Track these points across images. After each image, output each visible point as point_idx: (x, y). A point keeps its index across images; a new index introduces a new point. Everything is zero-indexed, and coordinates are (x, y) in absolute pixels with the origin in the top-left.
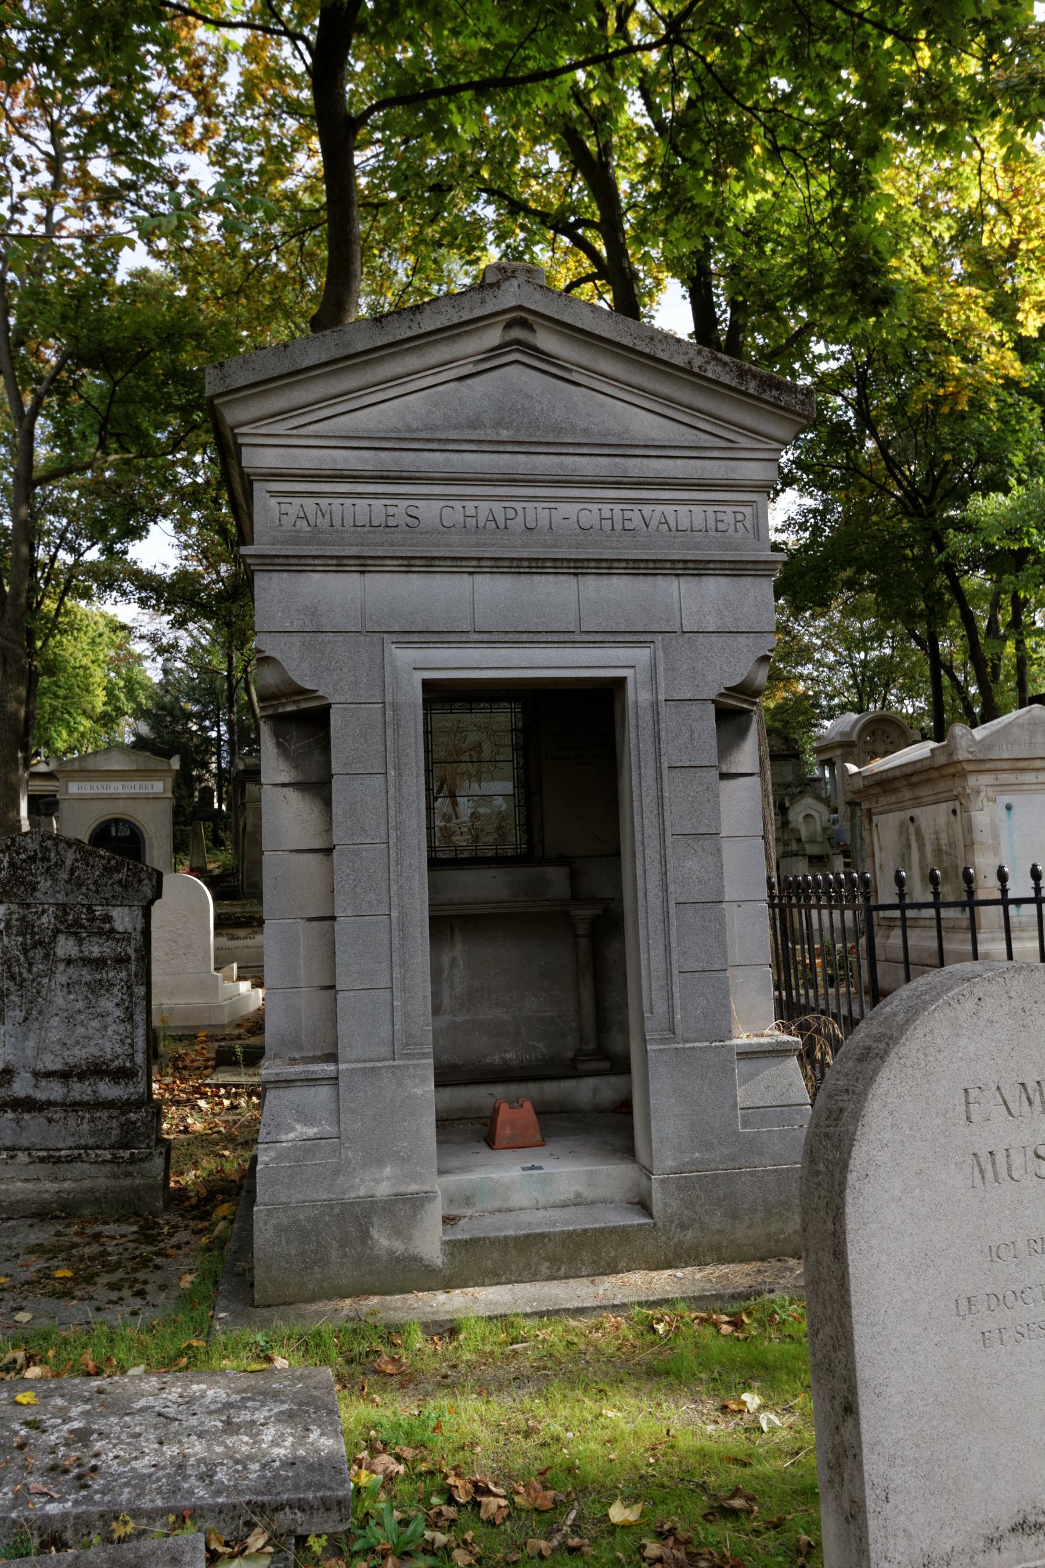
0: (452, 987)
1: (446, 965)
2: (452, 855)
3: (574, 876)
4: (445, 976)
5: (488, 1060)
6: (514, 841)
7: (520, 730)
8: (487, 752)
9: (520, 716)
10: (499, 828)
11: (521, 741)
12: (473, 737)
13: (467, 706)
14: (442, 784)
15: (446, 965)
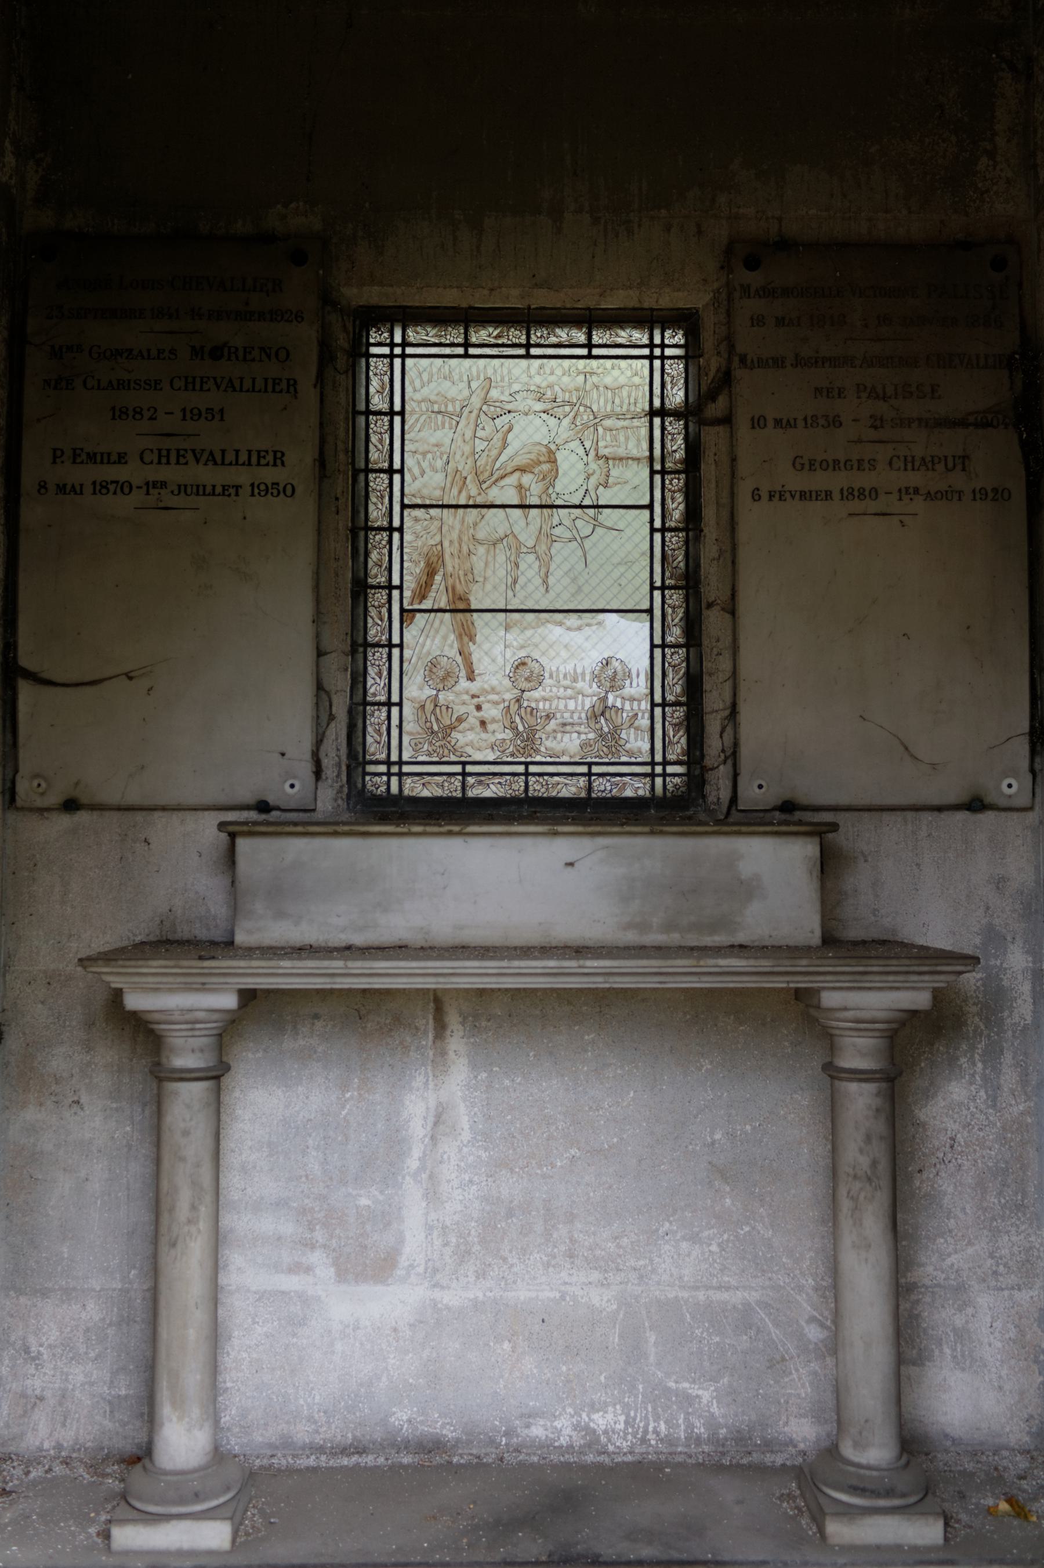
0: (433, 1196)
1: (418, 1129)
2: (452, 788)
3: (830, 864)
4: (413, 1163)
5: (538, 1431)
6: (643, 745)
7: (676, 414)
9: (676, 369)
10: (601, 711)
11: (677, 446)
12: (530, 432)
13: (517, 335)
15: (418, 1129)
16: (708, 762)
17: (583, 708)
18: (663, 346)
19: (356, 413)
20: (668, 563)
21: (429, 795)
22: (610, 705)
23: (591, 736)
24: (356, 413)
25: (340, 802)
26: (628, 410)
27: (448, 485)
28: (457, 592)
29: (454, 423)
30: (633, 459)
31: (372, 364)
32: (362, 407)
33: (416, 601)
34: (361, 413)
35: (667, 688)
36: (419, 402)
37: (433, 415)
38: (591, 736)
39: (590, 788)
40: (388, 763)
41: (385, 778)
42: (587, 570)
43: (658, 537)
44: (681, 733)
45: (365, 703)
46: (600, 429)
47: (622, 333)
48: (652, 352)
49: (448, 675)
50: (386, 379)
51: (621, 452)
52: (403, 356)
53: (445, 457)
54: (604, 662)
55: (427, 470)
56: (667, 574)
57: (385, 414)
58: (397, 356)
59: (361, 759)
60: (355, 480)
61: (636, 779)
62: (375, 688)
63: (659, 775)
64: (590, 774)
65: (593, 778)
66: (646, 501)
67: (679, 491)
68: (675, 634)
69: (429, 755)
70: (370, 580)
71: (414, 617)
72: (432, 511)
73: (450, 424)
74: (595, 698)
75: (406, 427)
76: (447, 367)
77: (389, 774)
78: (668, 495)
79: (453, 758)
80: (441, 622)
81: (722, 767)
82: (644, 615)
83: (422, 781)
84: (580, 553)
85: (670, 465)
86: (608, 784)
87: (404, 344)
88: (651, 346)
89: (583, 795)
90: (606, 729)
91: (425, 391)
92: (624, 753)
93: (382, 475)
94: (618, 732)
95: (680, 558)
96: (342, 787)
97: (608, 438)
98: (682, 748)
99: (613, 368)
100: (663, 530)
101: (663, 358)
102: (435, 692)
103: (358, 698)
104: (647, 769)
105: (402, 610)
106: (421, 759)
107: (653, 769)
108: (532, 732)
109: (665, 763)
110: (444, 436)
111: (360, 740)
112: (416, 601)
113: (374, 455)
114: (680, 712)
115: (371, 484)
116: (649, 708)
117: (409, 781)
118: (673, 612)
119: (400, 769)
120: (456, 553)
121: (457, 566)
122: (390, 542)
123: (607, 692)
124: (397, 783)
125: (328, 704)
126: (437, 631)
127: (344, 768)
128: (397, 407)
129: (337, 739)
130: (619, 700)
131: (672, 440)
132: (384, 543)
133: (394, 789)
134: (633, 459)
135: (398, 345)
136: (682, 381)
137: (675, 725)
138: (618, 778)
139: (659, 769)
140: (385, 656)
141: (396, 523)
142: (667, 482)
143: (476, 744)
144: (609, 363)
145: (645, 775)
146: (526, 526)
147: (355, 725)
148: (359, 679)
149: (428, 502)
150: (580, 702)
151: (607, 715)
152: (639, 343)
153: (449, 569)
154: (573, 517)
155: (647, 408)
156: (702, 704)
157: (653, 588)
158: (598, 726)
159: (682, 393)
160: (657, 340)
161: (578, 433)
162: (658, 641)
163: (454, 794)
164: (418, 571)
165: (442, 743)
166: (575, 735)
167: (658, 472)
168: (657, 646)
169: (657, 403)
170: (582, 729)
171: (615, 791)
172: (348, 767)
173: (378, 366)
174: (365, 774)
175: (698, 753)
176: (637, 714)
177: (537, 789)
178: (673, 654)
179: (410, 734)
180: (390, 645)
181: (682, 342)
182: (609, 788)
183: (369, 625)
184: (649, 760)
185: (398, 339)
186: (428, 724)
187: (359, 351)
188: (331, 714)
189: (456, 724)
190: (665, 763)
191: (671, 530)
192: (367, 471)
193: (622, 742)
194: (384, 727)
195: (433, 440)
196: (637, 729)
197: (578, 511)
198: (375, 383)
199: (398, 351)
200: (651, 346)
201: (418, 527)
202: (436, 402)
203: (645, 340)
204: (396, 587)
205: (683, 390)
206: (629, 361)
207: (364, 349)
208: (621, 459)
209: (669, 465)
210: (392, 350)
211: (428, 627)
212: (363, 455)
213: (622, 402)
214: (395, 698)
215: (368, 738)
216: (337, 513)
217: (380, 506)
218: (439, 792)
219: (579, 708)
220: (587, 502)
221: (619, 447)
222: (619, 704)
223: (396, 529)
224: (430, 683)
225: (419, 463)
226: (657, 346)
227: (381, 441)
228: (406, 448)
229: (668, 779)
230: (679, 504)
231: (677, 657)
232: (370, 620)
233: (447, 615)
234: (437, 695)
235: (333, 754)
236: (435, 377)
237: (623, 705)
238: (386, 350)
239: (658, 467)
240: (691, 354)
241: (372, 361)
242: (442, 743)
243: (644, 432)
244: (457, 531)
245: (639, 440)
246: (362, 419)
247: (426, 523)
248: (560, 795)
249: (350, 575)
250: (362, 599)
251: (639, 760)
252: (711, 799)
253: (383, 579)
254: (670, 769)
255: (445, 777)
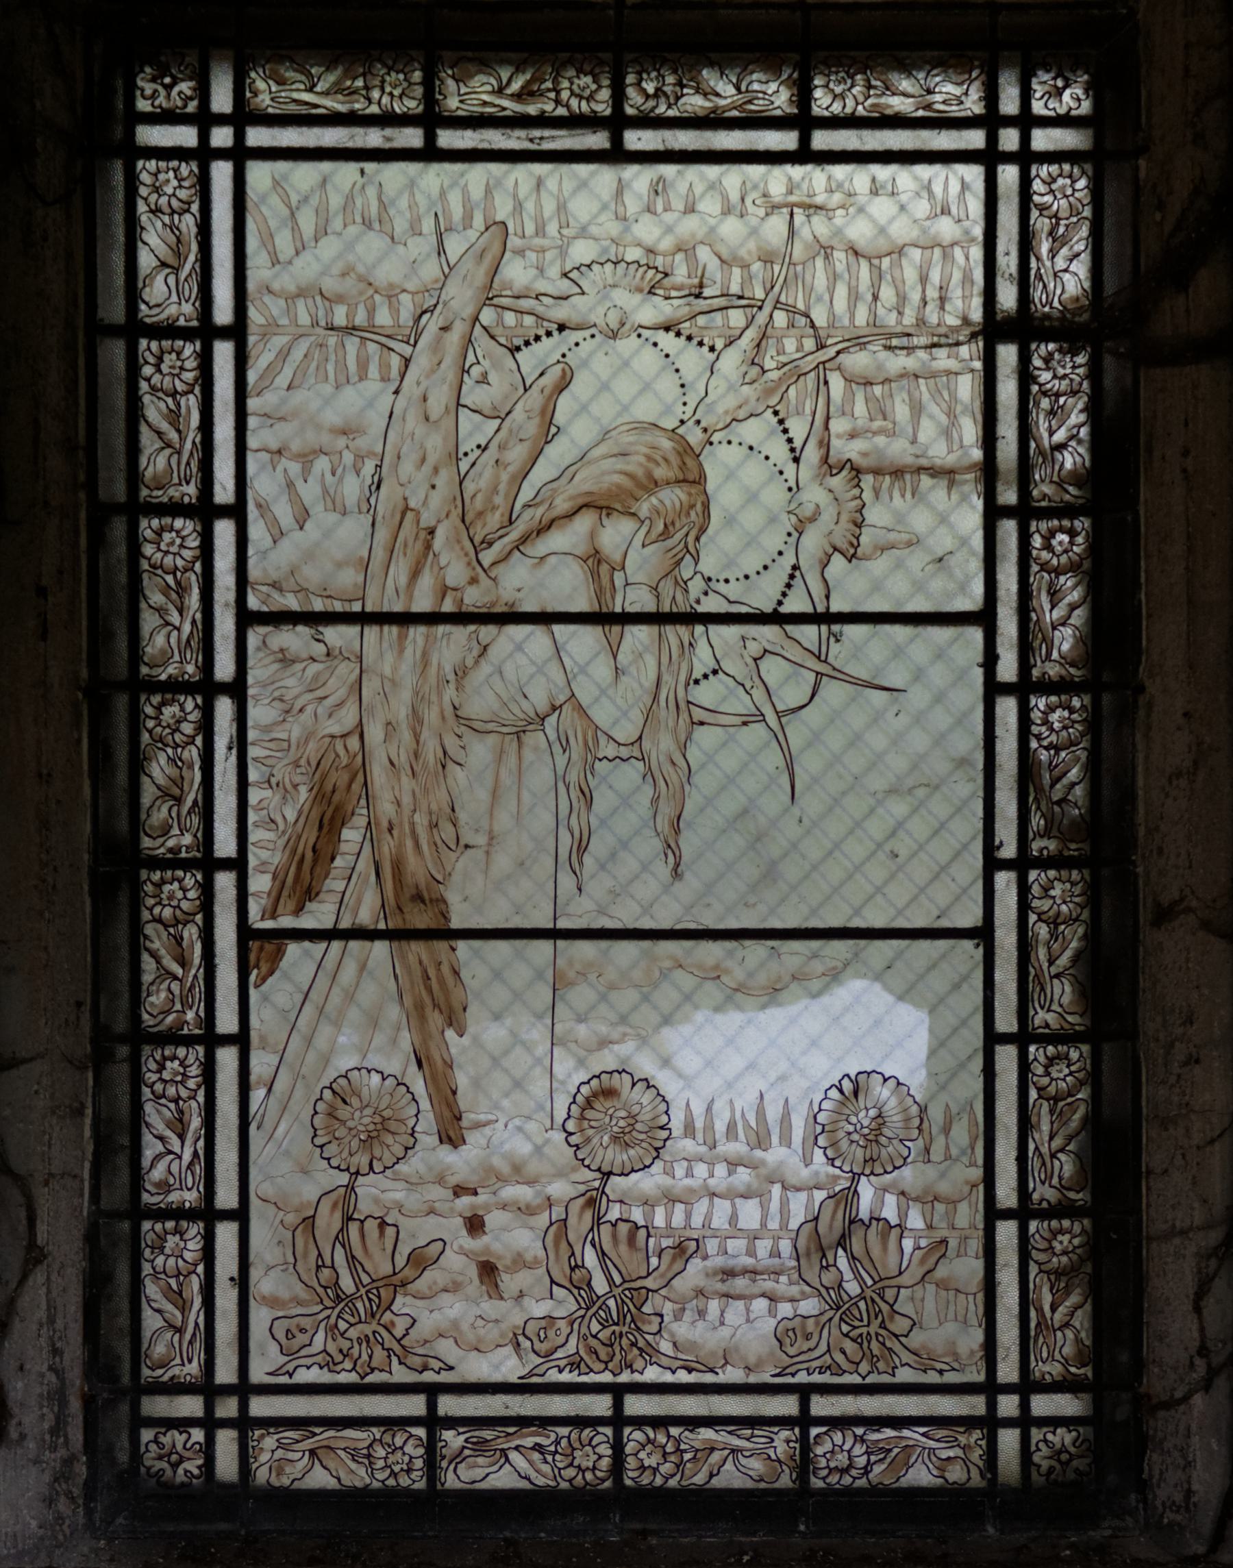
7: (1067, 330)
8: (744, 546)
9: (1064, 193)
10: (837, 1234)
11: (1067, 434)
12: (627, 388)
13: (585, 92)
14: (329, 818)
16: (1156, 1383)
17: (784, 1225)
18: (1026, 121)
19: (99, 330)
20: (1039, 789)
21: (332, 1483)
22: (864, 1214)
23: (809, 1306)
24: (99, 330)
25: (63, 1505)
26: (921, 322)
27: (379, 554)
28: (409, 880)
29: (395, 361)
30: (935, 472)
31: (145, 177)
32: (115, 311)
33: (287, 904)
34: (113, 331)
35: (1034, 1163)
36: (291, 298)
37: (332, 340)
38: (809, 1306)
39: (804, 1462)
40: (208, 1388)
41: (198, 1435)
42: (796, 811)
43: (1007, 708)
44: (1074, 1299)
45: (138, 1213)
46: (836, 383)
47: (905, 85)
48: (992, 139)
49: (383, 1125)
50: (188, 224)
51: (898, 450)
52: (240, 155)
53: (369, 467)
54: (847, 1086)
55: (317, 510)
56: (1037, 822)
57: (186, 334)
58: (222, 154)
59: (126, 1379)
60: (98, 540)
61: (941, 1433)
62: (166, 1163)
63: (1009, 1423)
64: (804, 1420)
65: (814, 1431)
66: (972, 599)
67: (1073, 567)
68: (1060, 1002)
69: (330, 1364)
70: (146, 842)
71: (279, 954)
72: (335, 635)
73: (384, 366)
74: (820, 1195)
75: (252, 377)
76: (371, 192)
77: (210, 1423)
78: (1040, 580)
79: (400, 1375)
80: (363, 967)
81: (1198, 1399)
82: (968, 944)
83: (308, 1444)
84: (774, 758)
85: (1047, 489)
86: (859, 1450)
87: (243, 116)
88: (991, 121)
89: (786, 1481)
90: (853, 1288)
91: (306, 268)
92: (906, 1357)
93: (179, 523)
94: (890, 1294)
95: (1074, 774)
96: (69, 1462)
97: (860, 408)
98: (1078, 1340)
99: (875, 192)
100: (1024, 688)
101: (1026, 158)
102: (344, 1178)
103: (115, 1197)
104: (975, 1405)
105: (245, 933)
106: (305, 1376)
107: (992, 1405)
108: (633, 1295)
109: (1027, 1386)
110: (364, 400)
111: (124, 1321)
112: (287, 904)
113: (154, 462)
114: (1068, 1238)
115: (148, 550)
116: (980, 1218)
117: (270, 1442)
118: (1054, 935)
119: (244, 1406)
120: (403, 759)
121: (406, 800)
122: (206, 726)
123: (855, 1177)
124: (234, 1448)
125: (23, 1214)
126: (350, 997)
127: (75, 1405)
128: (223, 314)
129: (51, 1320)
130: (891, 1199)
131: (1052, 413)
132: (188, 728)
133: (227, 1466)
134: (935, 472)
135: (222, 120)
136: (1084, 231)
137: (1058, 1273)
138: (889, 1433)
139: (1008, 1405)
140: (194, 1071)
141: (224, 668)
142: (1037, 541)
143: (473, 1334)
144: (859, 177)
145: (968, 1422)
146: (609, 679)
147: (109, 1278)
148: (118, 1141)
149: (318, 605)
150: (775, 1205)
151: (857, 1246)
152: (954, 111)
153: (386, 808)
154: (754, 648)
155: (977, 315)
156: (1139, 1211)
157: (992, 864)
158: (829, 1278)
159: (1081, 267)
160: (1009, 104)
161: (769, 392)
162: (1006, 1022)
163: (404, 1481)
164: (291, 815)
165: (367, 1329)
166: (760, 1305)
167: (1008, 512)
168: (1006, 1039)
169: (1007, 297)
170: (783, 1285)
171: (878, 1469)
172: (88, 1402)
173: (165, 184)
174: (139, 1421)
175: (1124, 1357)
176: (944, 1242)
177: (648, 1462)
178: (1051, 1061)
179: (272, 1302)
180: (211, 1039)
181: (1085, 107)
182: (861, 1461)
183: (147, 978)
184: (981, 1378)
185: (222, 101)
186: (326, 1272)
187: (107, 141)
188: (32, 1245)
189: (409, 1273)
190: (1027, 1386)
191: (1046, 687)
192: (136, 509)
193: (900, 1325)
194: (195, 1283)
195: (331, 417)
196: (942, 1285)
197: (768, 633)
198: (154, 241)
199: (222, 137)
200: (991, 121)
201: (292, 683)
202: (340, 299)
203: (973, 105)
204: (226, 864)
205: (1085, 257)
206: (923, 171)
207: (119, 132)
208: (897, 473)
209: (1043, 489)
210: (204, 137)
211: (322, 983)
212: (121, 461)
213: (902, 298)
214: (227, 1197)
215: (147, 1313)
216: (44, 637)
217: (175, 618)
218: (358, 1476)
219: (774, 1225)
220: (794, 605)
221: (892, 434)
222: (890, 1212)
223: (224, 688)
224: (331, 1150)
225: (290, 485)
226: (1009, 121)
227: (174, 417)
228: (252, 442)
229: (1036, 1434)
230: (1073, 607)
231: (1064, 1072)
232: (148, 963)
233: (380, 949)
234: (350, 1188)
235: (39, 1364)
236: (337, 224)
237: (903, 1215)
238: (186, 136)
239: (1008, 496)
240: (1109, 153)
241: (146, 169)
242: (367, 1329)
243: (967, 388)
244: (406, 695)
245: (951, 414)
246: (115, 351)
247: (314, 668)
248: (716, 1483)
249: (88, 827)
250: (124, 899)
251: (951, 1378)
252: (1166, 1492)
253: (187, 839)
254: (1042, 1405)
255: (377, 1432)
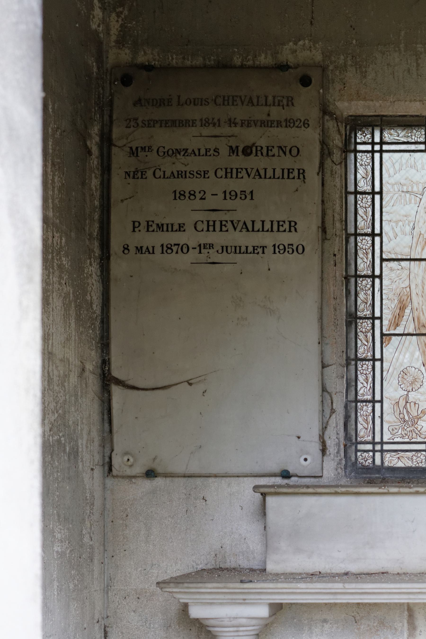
19: (347, 193)
21: (403, 466)
24: (347, 193)
25: (339, 470)
27: (414, 245)
28: (421, 322)
29: (418, 199)
31: (359, 157)
32: (351, 188)
33: (392, 328)
34: (351, 193)
36: (393, 185)
37: (403, 194)
41: (371, 454)
45: (356, 401)
50: (369, 168)
52: (381, 151)
53: (412, 225)
55: (399, 234)
57: (368, 193)
58: (377, 151)
59: (354, 441)
60: (347, 241)
62: (364, 390)
69: (403, 437)
70: (359, 313)
71: (390, 339)
72: (403, 263)
73: (415, 200)
75: (384, 203)
76: (412, 159)
77: (374, 451)
79: (419, 440)
80: (410, 343)
83: (398, 456)
87: (382, 143)
91: (398, 177)
93: (367, 238)
96: (341, 460)
102: (406, 393)
103: (352, 397)
105: (382, 335)
106: (396, 440)
110: (411, 209)
111: (353, 427)
112: (392, 328)
113: (361, 223)
115: (359, 244)
117: (388, 455)
119: (382, 447)
120: (420, 294)
121: (421, 303)
122: (373, 286)
124: (380, 457)
125: (330, 401)
126: (407, 349)
127: (342, 447)
129: (337, 427)
132: (369, 286)
133: (378, 462)
135: (377, 143)
140: (370, 367)
141: (377, 272)
147: (350, 417)
148: (352, 384)
149: (400, 257)
153: (415, 305)
163: (420, 465)
164: (393, 307)
165: (412, 429)
172: (345, 446)
173: (363, 159)
174: (357, 451)
179: (389, 422)
180: (374, 360)
183: (359, 345)
185: (377, 139)
186: (401, 415)
188: (332, 409)
189: (421, 415)
192: (356, 235)
194: (370, 418)
195: (403, 212)
198: (361, 171)
199: (377, 147)
201: (393, 275)
202: (405, 185)
204: (377, 318)
207: (353, 147)
210: (373, 147)
211: (401, 346)
212: (353, 223)
214: (378, 397)
215: (359, 425)
216: (335, 266)
218: (409, 464)
223: (377, 277)
224: (402, 386)
225: (393, 229)
227: (366, 213)
228: (384, 218)
232: (359, 342)
233: (414, 338)
234: (407, 395)
235: (334, 437)
236: (404, 167)
238: (369, 147)
241: (359, 155)
242: (412, 429)
244: (421, 278)
247: (399, 272)
249: (345, 310)
250: (353, 326)
253: (368, 312)
255: (414, 453)
